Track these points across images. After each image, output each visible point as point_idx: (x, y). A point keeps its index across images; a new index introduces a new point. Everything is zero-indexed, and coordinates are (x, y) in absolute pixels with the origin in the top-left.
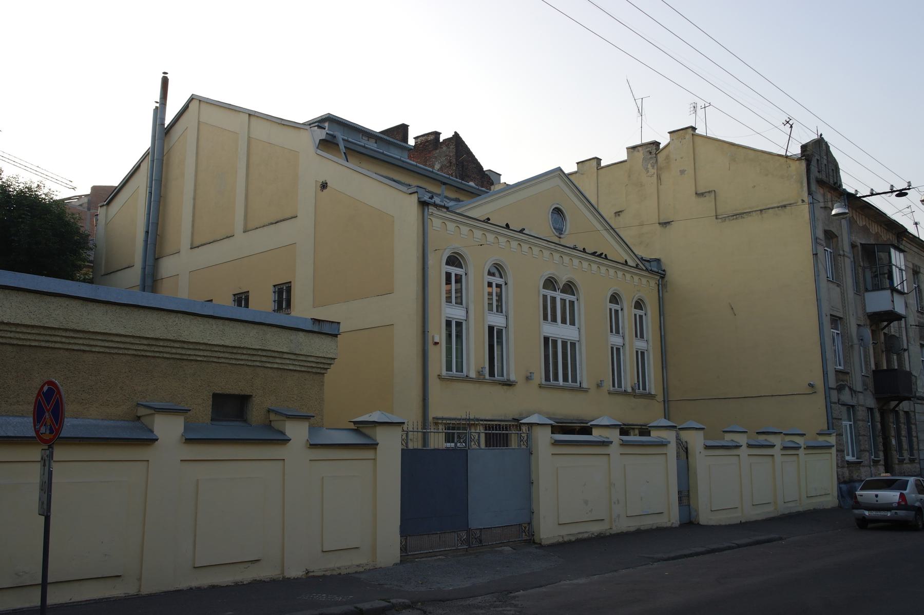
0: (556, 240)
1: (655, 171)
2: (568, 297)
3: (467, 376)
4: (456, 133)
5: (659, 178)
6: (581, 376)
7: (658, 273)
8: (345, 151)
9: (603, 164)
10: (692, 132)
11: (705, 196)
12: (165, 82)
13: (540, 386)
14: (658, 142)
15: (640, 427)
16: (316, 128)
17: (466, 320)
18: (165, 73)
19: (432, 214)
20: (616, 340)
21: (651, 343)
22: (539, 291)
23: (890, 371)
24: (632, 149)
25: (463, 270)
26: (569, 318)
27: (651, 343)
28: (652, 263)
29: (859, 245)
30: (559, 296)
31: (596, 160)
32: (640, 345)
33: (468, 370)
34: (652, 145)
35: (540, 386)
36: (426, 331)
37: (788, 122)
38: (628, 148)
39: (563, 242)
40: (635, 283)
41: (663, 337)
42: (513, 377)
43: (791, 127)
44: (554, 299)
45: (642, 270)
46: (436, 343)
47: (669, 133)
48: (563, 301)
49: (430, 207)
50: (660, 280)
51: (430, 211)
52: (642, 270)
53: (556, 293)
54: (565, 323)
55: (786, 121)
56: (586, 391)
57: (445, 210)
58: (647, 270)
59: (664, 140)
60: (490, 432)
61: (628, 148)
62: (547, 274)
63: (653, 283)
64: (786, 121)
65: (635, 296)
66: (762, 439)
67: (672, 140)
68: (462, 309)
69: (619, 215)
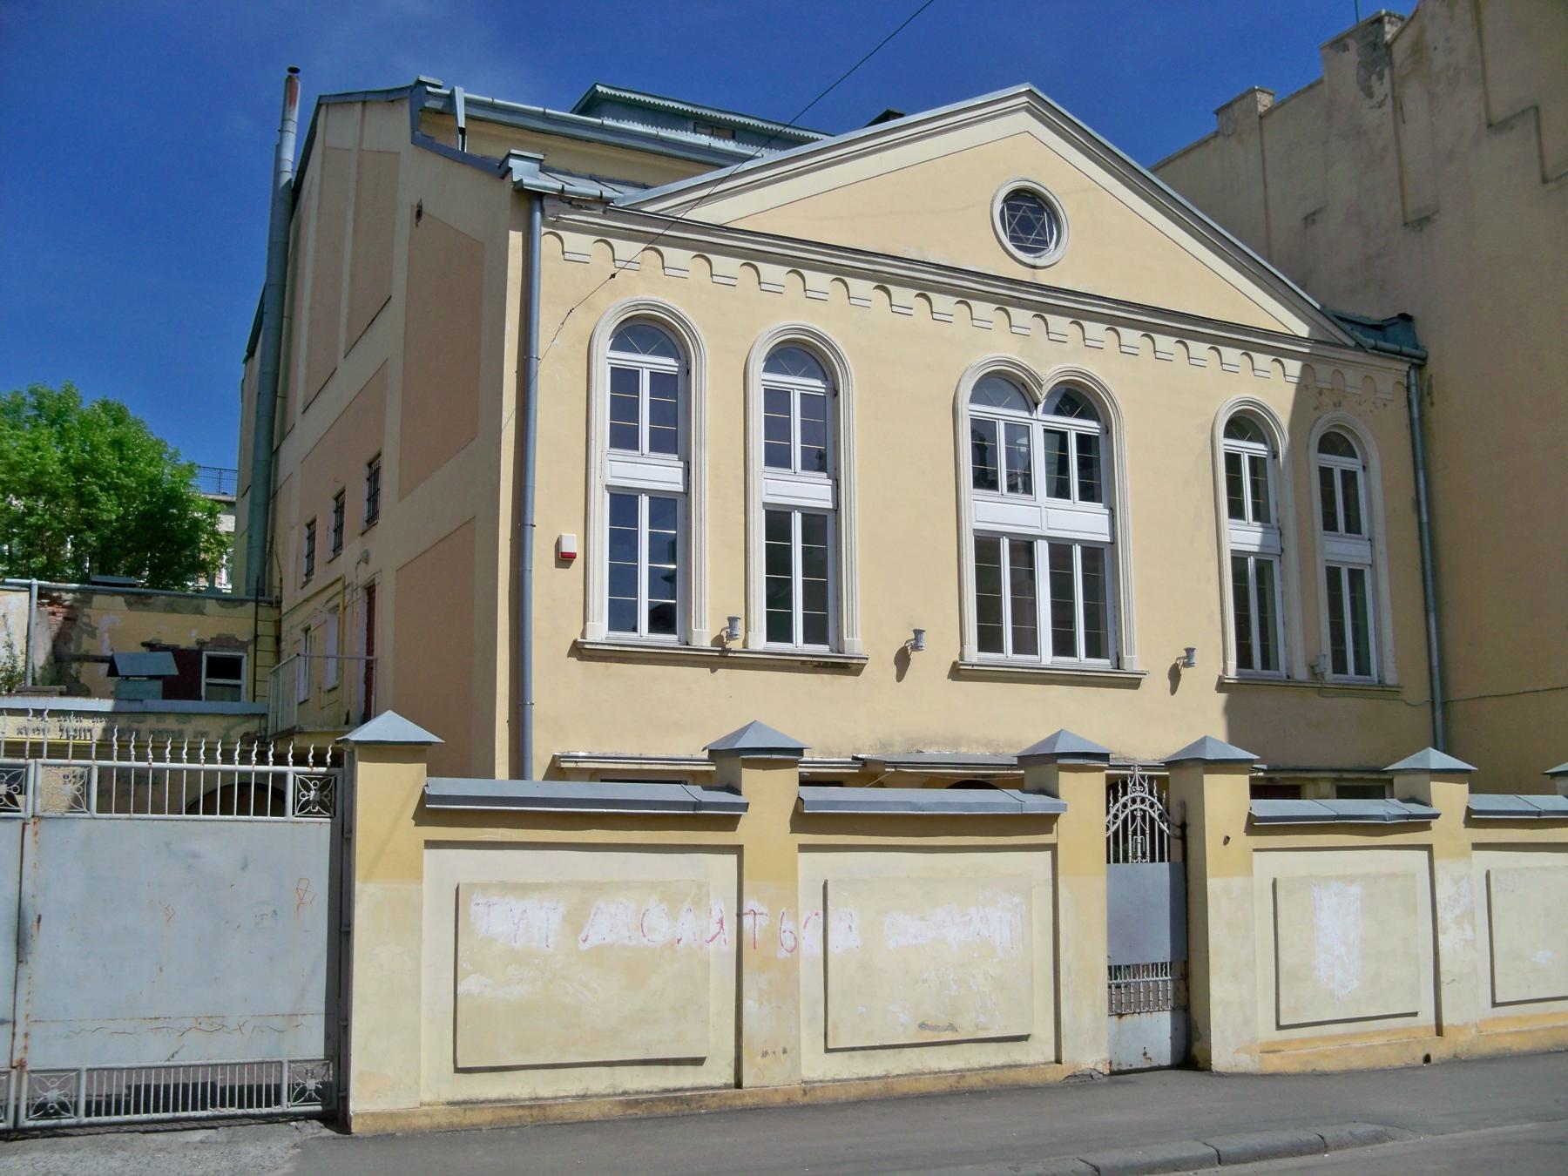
0: (1024, 274)
11: (1512, 128)
15: (1334, 775)
27: (1381, 545)
30: (1040, 422)
32: (1345, 550)
39: (1043, 278)
40: (1320, 385)
41: (1425, 528)
45: (1345, 346)
48: (1057, 439)
49: (546, 202)
50: (1412, 373)
52: (1345, 346)
58: (1359, 346)
60: (144, 764)
69: (1314, 221)
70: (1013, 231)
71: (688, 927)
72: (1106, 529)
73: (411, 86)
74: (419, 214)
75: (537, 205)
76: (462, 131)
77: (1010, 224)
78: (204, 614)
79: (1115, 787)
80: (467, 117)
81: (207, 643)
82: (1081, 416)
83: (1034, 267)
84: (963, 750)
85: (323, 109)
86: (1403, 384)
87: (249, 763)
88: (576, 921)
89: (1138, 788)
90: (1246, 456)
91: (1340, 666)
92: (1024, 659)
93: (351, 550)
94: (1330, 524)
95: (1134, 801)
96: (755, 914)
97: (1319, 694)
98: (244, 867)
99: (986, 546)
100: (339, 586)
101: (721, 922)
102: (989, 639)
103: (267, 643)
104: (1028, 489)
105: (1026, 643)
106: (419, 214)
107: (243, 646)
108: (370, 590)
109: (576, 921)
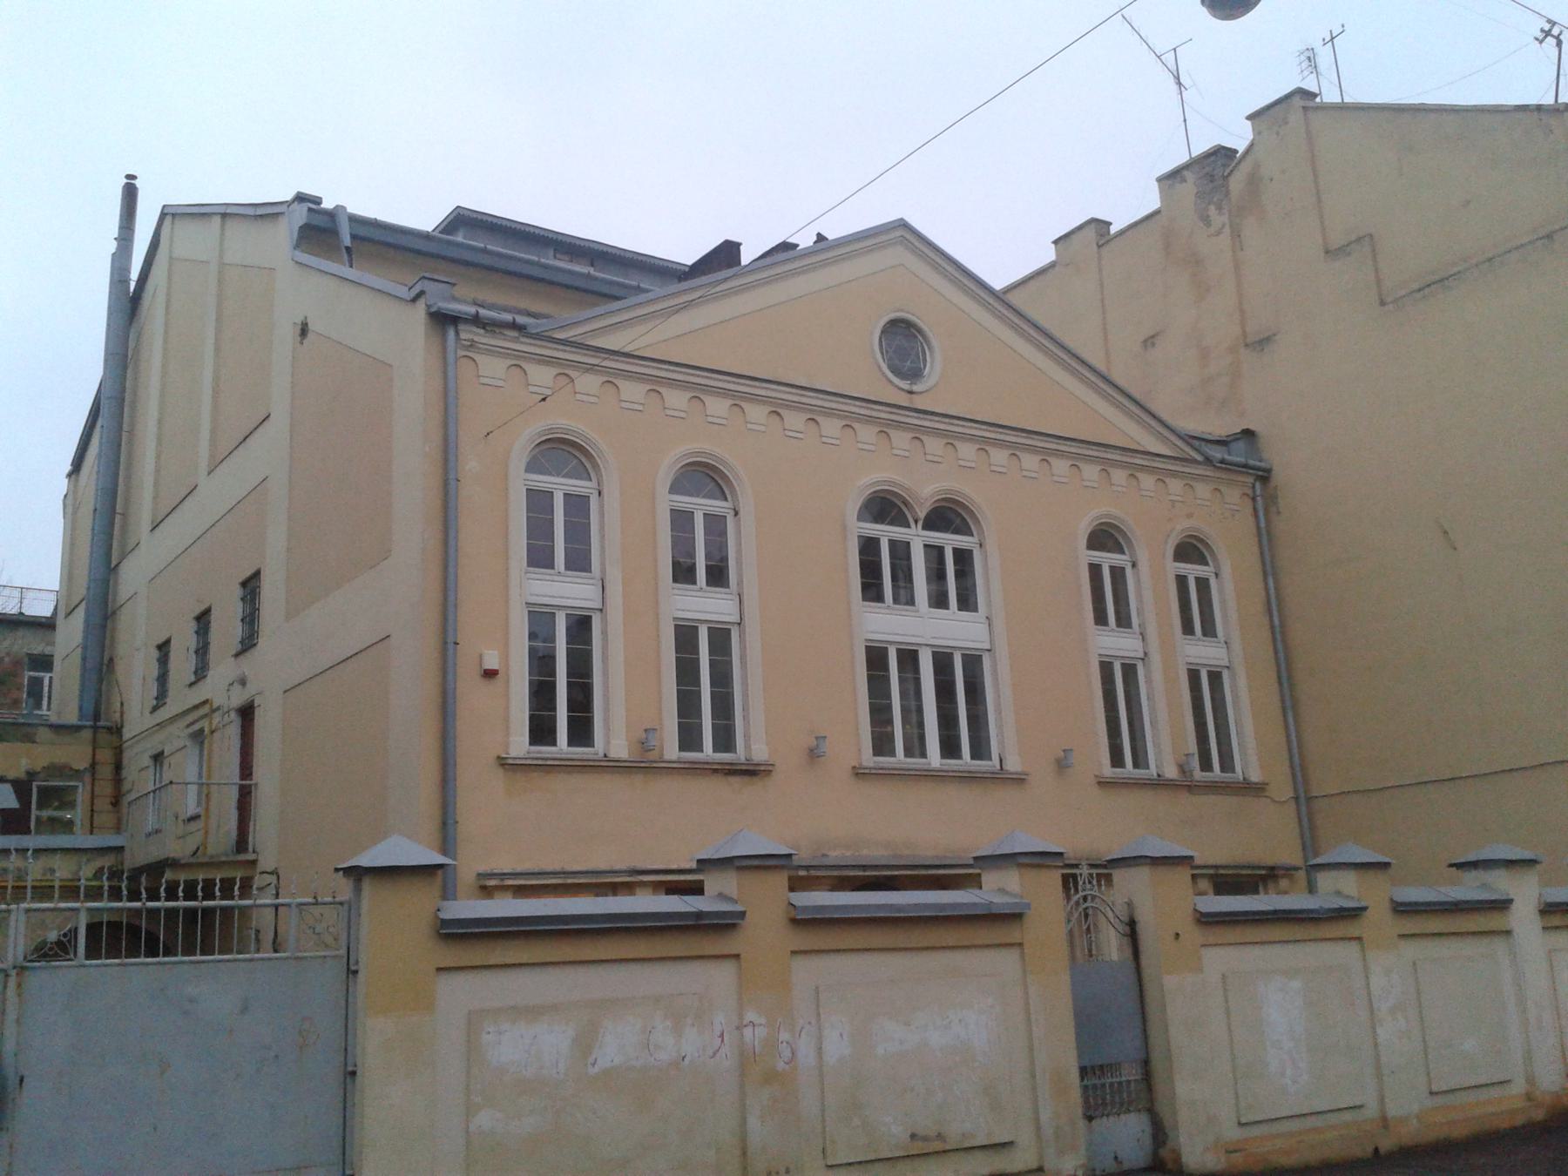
0: (903, 400)
1: (1225, 218)
2: (949, 541)
3: (605, 756)
5: (1236, 235)
6: (1001, 743)
7: (1245, 466)
8: (349, 245)
9: (1113, 229)
10: (1302, 103)
12: (130, 194)
13: (859, 773)
14: (1230, 149)
16: (296, 203)
18: (131, 177)
19: (472, 345)
20: (1117, 643)
21: (1237, 646)
22: (844, 527)
24: (1171, 179)
25: (593, 484)
28: (1234, 446)
30: (918, 539)
31: (1093, 225)
32: (1203, 652)
33: (608, 743)
34: (1213, 158)
35: (859, 773)
36: (450, 640)
38: (1159, 180)
39: (919, 403)
42: (760, 753)
44: (901, 552)
45: (1195, 461)
46: (490, 674)
47: (1249, 118)
48: (935, 554)
51: (463, 336)
52: (1195, 461)
54: (879, 598)
56: (1019, 780)
57: (514, 334)
58: (1208, 461)
59: (1239, 137)
60: (137, 904)
61: (1159, 180)
63: (1234, 495)
66: (1468, 888)
67: (1257, 132)
68: (591, 581)
69: (1153, 345)
70: (890, 359)
71: (692, 1042)
72: (986, 637)
73: (287, 202)
74: (304, 331)
75: (451, 333)
76: (347, 249)
77: (887, 352)
78: (34, 742)
79: (1069, 882)
80: (354, 237)
81: (39, 773)
82: (956, 532)
83: (911, 392)
84: (865, 852)
85: (168, 220)
86: (1248, 495)
87: (176, 899)
88: (585, 1044)
89: (1088, 886)
90: (1107, 565)
91: (1206, 765)
92: (916, 762)
93: (222, 669)
94: (1188, 629)
95: (1085, 898)
96: (754, 1026)
98: (244, 1010)
99: (876, 657)
100: (206, 709)
101: (722, 1035)
102: (882, 744)
103: (106, 771)
104: (911, 601)
105: (916, 746)
106: (304, 331)
107: (77, 774)
108: (247, 713)
109: (585, 1044)
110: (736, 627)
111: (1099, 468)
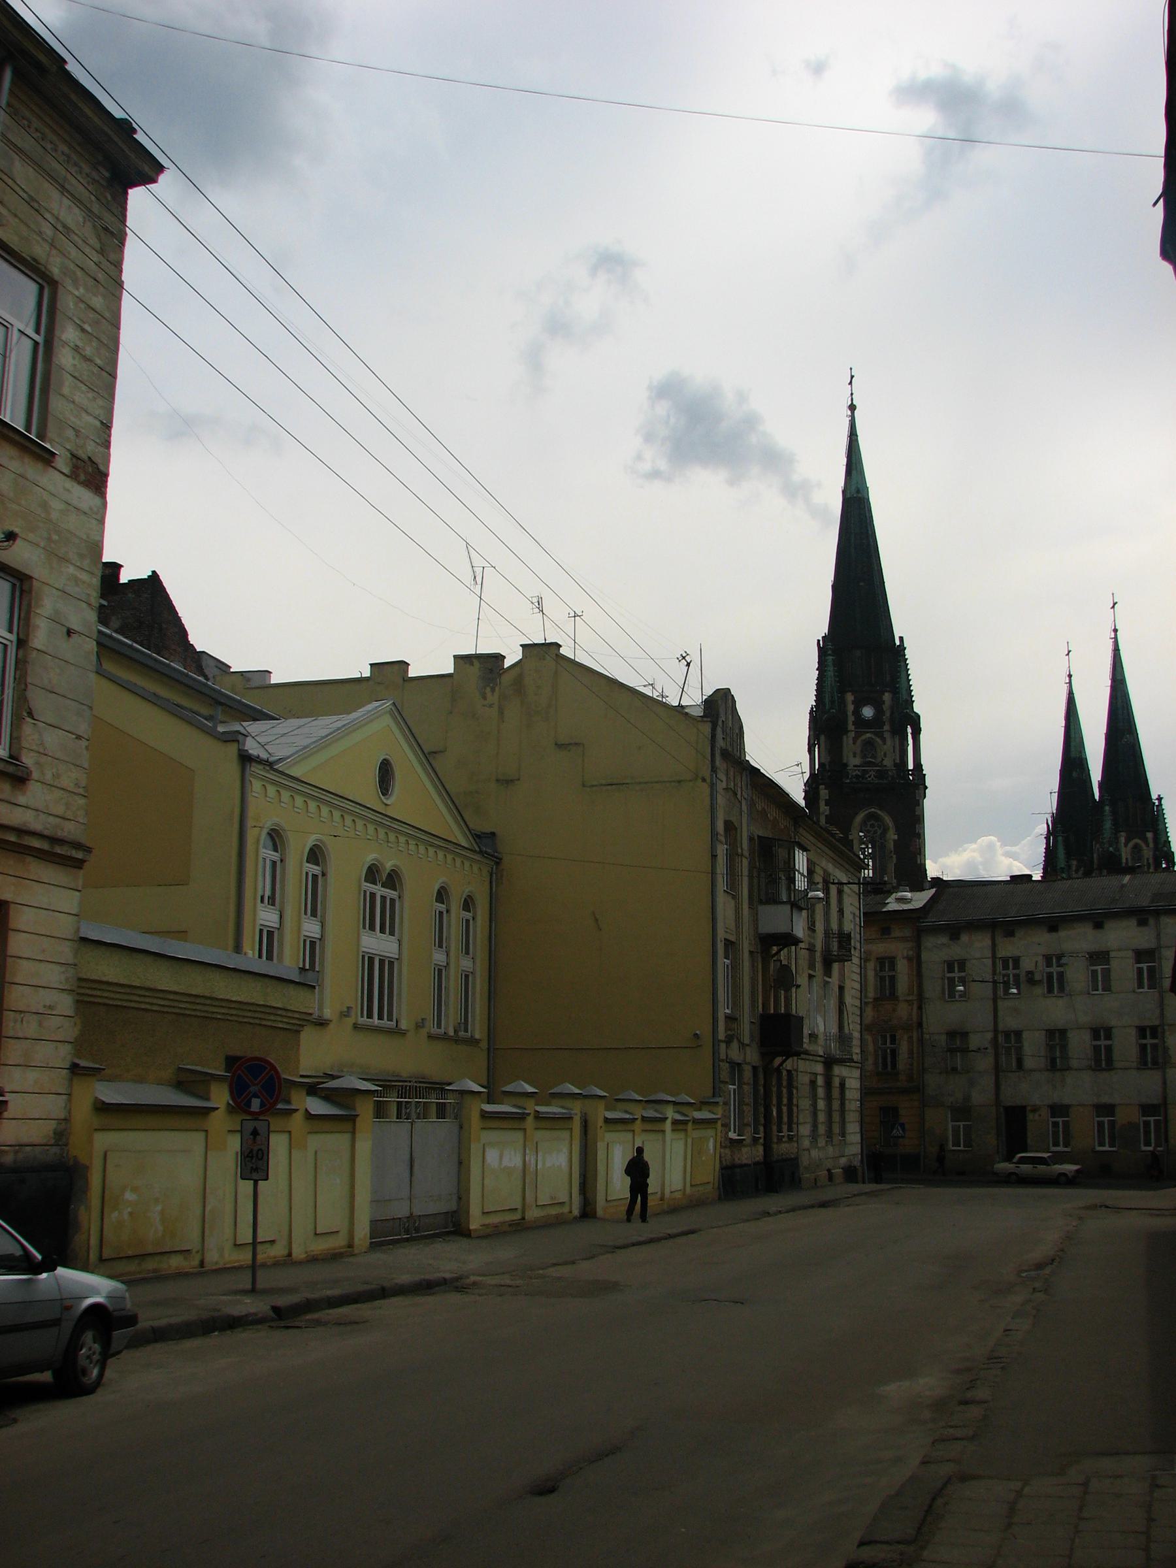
4: (154, 572)
9: (412, 673)
14: (502, 655)
17: (279, 929)
23: (777, 1016)
26: (390, 927)
29: (756, 838)
30: (379, 890)
37: (684, 658)
43: (688, 665)
50: (494, 867)
53: (376, 887)
55: (681, 655)
59: (513, 656)
62: (370, 858)
64: (681, 655)
65: (464, 892)
72: (397, 952)
97: (456, 1042)
110: (319, 941)
111: (405, 839)
